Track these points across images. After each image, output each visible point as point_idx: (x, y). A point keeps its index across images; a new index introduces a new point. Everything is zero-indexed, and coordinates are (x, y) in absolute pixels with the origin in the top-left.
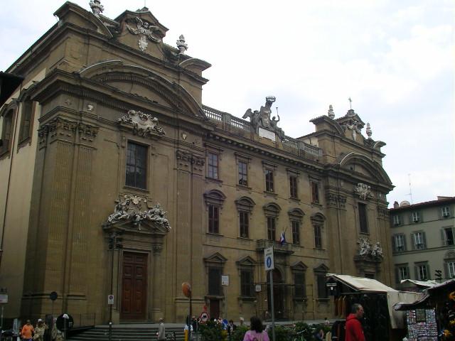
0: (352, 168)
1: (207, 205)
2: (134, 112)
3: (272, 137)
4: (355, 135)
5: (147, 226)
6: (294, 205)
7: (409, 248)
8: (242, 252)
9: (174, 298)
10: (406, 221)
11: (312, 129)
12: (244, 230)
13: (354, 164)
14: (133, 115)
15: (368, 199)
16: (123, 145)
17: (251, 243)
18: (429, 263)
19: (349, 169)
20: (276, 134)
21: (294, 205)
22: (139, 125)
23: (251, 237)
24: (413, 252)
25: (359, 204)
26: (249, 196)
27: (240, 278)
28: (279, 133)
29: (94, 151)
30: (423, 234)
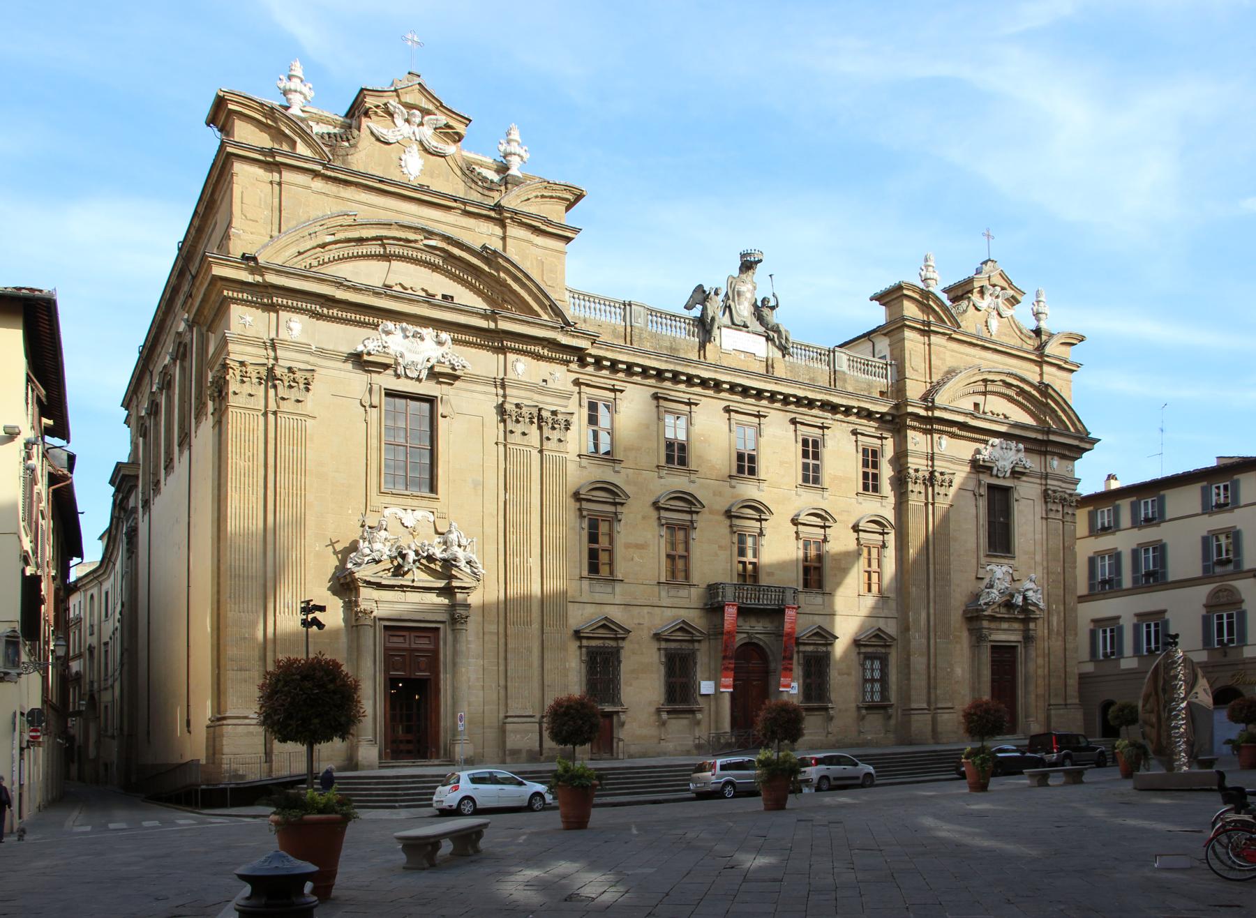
0: (976, 405)
1: (582, 517)
2: (390, 325)
3: (759, 346)
4: (994, 323)
5: (428, 570)
6: (808, 500)
7: (1127, 582)
8: (669, 613)
9: (502, 715)
10: (1125, 519)
11: (878, 315)
12: (679, 566)
13: (985, 393)
14: (388, 333)
15: (1016, 474)
16: (375, 401)
17: (693, 590)
18: (1167, 616)
19: (971, 408)
20: (768, 339)
21: (808, 500)
22: (406, 354)
23: (696, 577)
24: (1137, 589)
25: (991, 487)
26: (690, 489)
27: (662, 669)
28: (773, 334)
29: (310, 422)
30: (1160, 549)
